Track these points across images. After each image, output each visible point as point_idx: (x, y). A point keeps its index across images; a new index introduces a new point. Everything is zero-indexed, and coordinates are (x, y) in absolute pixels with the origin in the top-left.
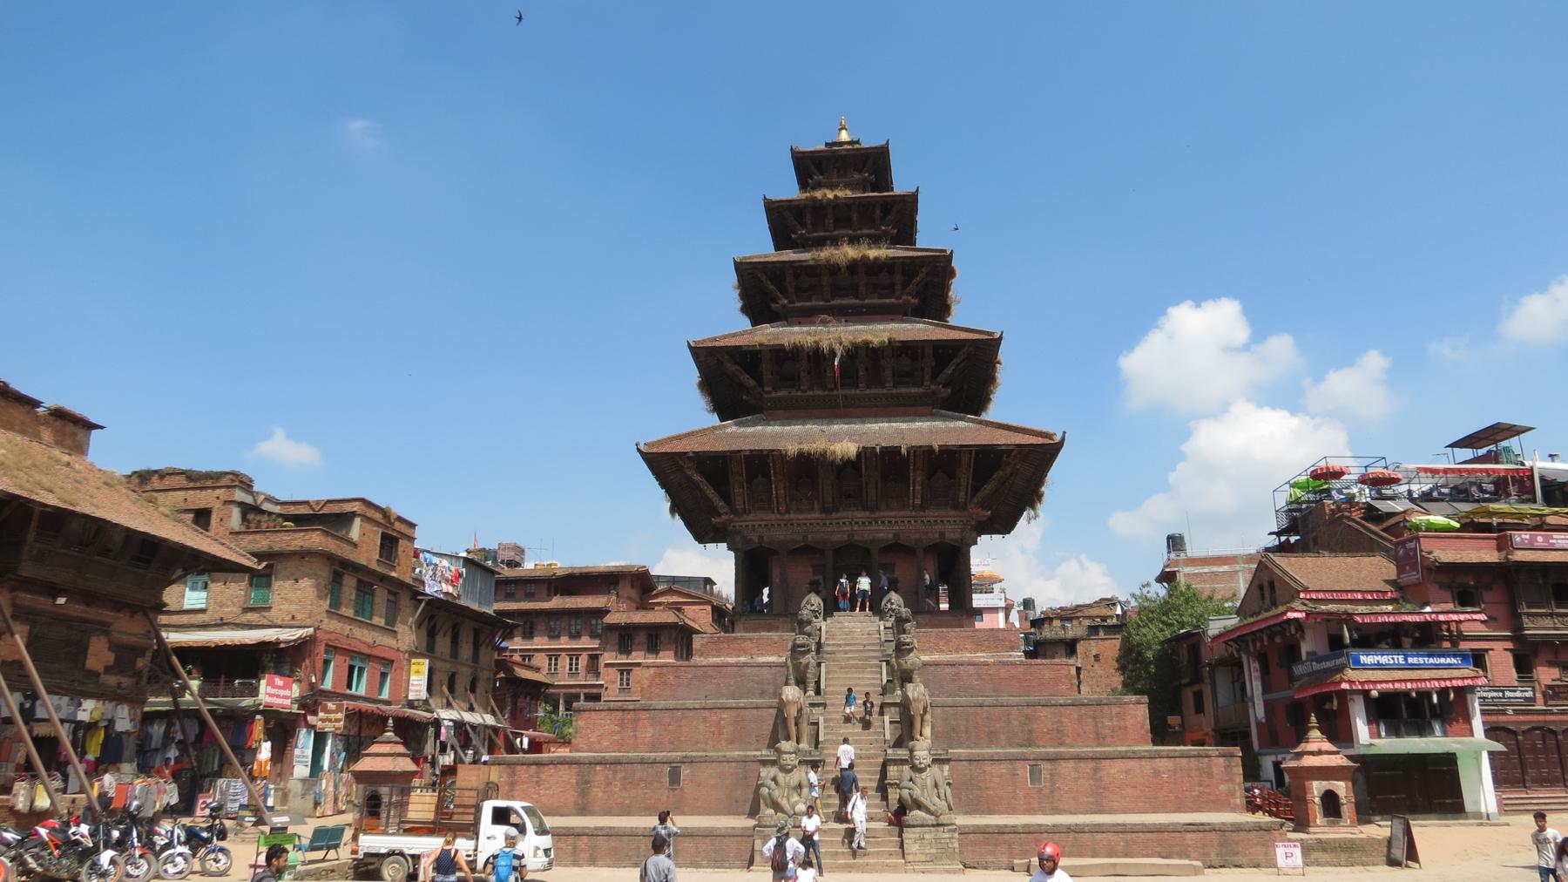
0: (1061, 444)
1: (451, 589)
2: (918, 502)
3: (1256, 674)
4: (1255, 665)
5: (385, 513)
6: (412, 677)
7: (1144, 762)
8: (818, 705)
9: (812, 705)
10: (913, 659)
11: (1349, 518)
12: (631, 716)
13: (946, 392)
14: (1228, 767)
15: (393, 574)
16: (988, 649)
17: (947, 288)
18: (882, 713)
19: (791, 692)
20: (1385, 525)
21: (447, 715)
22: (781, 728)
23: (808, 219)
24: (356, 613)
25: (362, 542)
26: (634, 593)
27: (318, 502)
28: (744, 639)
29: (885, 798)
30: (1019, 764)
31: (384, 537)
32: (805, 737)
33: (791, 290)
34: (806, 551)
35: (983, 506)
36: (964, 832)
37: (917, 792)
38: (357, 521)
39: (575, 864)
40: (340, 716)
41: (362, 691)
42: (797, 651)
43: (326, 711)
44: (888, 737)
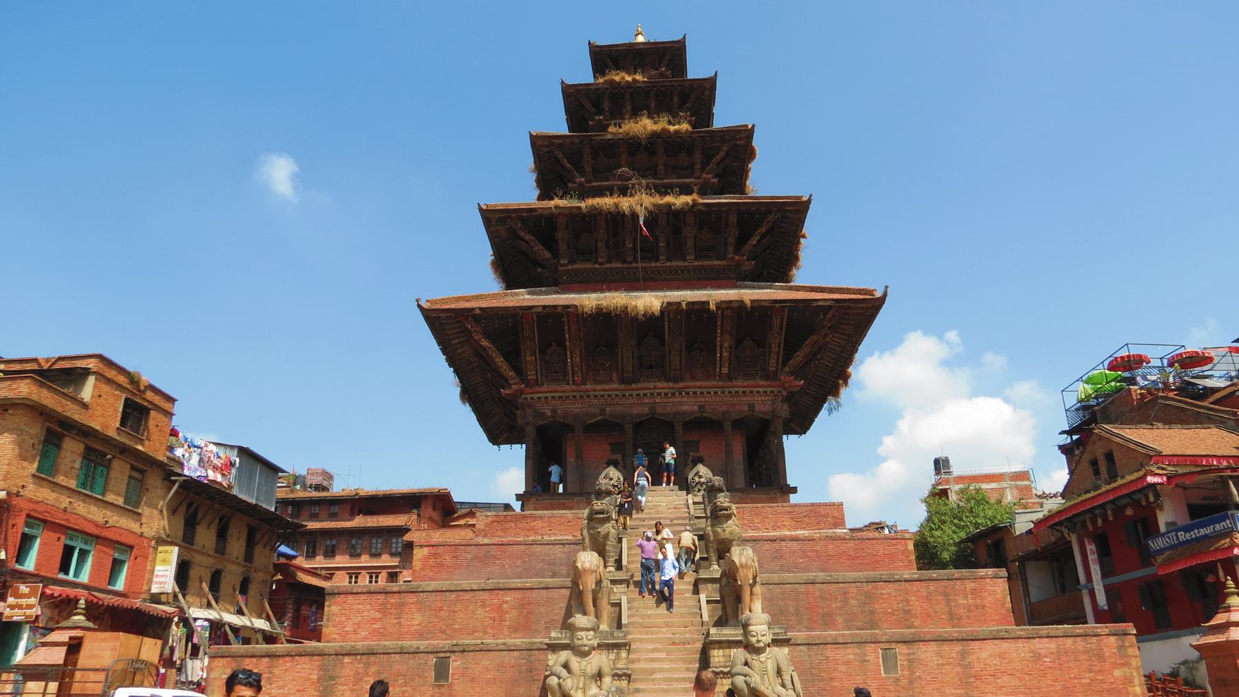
0: (882, 300)
1: (219, 478)
2: (725, 370)
3: (1092, 557)
4: (1091, 547)
5: (133, 379)
6: (157, 568)
7: (1020, 643)
8: (620, 582)
9: (614, 582)
10: (731, 527)
11: (1166, 398)
12: (394, 600)
13: (749, 265)
14: (1121, 647)
15: (140, 447)
18: (696, 591)
19: (588, 559)
20: (1211, 400)
21: (200, 615)
22: (576, 600)
23: (606, 105)
24: (84, 485)
25: (98, 407)
27: (47, 360)
30: (869, 648)
31: (128, 404)
32: (605, 617)
33: (588, 169)
34: (605, 427)
35: (798, 373)
37: (756, 680)
38: (91, 380)
40: (33, 601)
41: (84, 578)
42: (596, 519)
43: (17, 595)
44: (706, 618)
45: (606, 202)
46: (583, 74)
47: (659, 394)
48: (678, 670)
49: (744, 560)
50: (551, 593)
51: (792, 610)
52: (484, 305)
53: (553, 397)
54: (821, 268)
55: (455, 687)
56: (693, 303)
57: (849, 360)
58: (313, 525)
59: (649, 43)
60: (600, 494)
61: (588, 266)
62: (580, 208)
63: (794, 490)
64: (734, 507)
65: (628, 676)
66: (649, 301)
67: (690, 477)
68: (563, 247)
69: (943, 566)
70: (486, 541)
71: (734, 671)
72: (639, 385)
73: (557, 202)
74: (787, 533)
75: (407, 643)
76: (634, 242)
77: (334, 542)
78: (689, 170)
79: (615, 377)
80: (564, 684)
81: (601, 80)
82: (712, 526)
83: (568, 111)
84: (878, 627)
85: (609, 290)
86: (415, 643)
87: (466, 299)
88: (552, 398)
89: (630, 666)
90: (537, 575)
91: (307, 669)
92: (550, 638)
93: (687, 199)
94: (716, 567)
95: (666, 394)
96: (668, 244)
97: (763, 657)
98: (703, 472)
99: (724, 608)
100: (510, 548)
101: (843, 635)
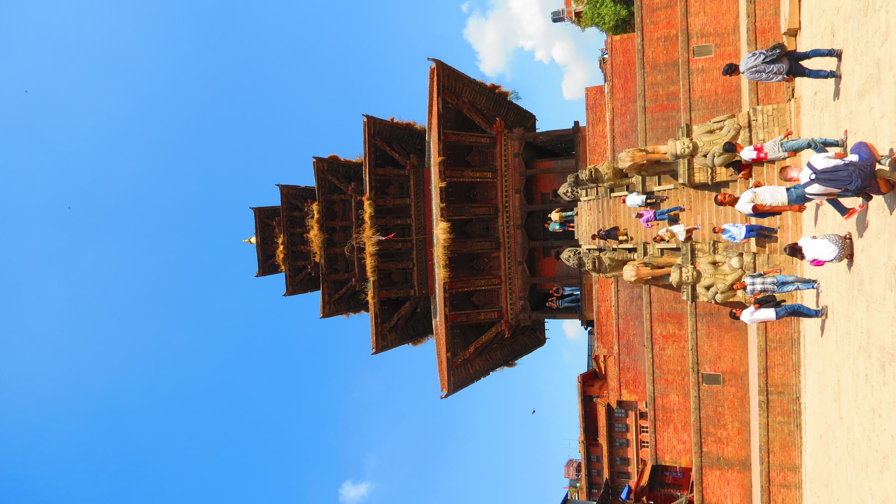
2: (490, 175)
8: (645, 249)
9: (645, 254)
10: (604, 169)
12: (660, 415)
13: (413, 158)
16: (603, 112)
17: (350, 162)
19: (629, 273)
22: (659, 281)
23: (301, 263)
26: (597, 385)
28: (599, 312)
30: (693, 67)
33: (346, 275)
35: (491, 122)
36: (757, 100)
37: (718, 149)
39: (799, 486)
42: (599, 267)
44: (671, 186)
45: (369, 263)
46: (279, 280)
47: (507, 222)
49: (628, 159)
50: (654, 299)
51: (665, 124)
52: (445, 350)
54: (414, 106)
55: (724, 369)
56: (441, 199)
57: (481, 86)
58: (606, 474)
59: (256, 234)
60: (581, 264)
61: (415, 276)
62: (374, 282)
63: (576, 123)
64: (589, 167)
65: (715, 242)
66: (440, 230)
67: (567, 199)
68: (402, 293)
69: (632, 14)
70: (616, 348)
71: (710, 165)
72: (501, 237)
73: (370, 298)
74: (608, 128)
75: (693, 406)
76: (398, 242)
77: (618, 459)
78: (346, 203)
79: (495, 255)
80: (721, 290)
81: (283, 268)
82: (603, 182)
83: (305, 291)
84: (677, 61)
85: (432, 259)
86: (692, 399)
87: (440, 363)
88: (511, 302)
89: (707, 240)
90: (641, 310)
91: (712, 478)
92: (688, 300)
93: (367, 204)
94: (634, 179)
95: (507, 217)
96: (399, 217)
97: (700, 144)
98: (564, 189)
99: (664, 173)
100: (621, 329)
101: (683, 85)
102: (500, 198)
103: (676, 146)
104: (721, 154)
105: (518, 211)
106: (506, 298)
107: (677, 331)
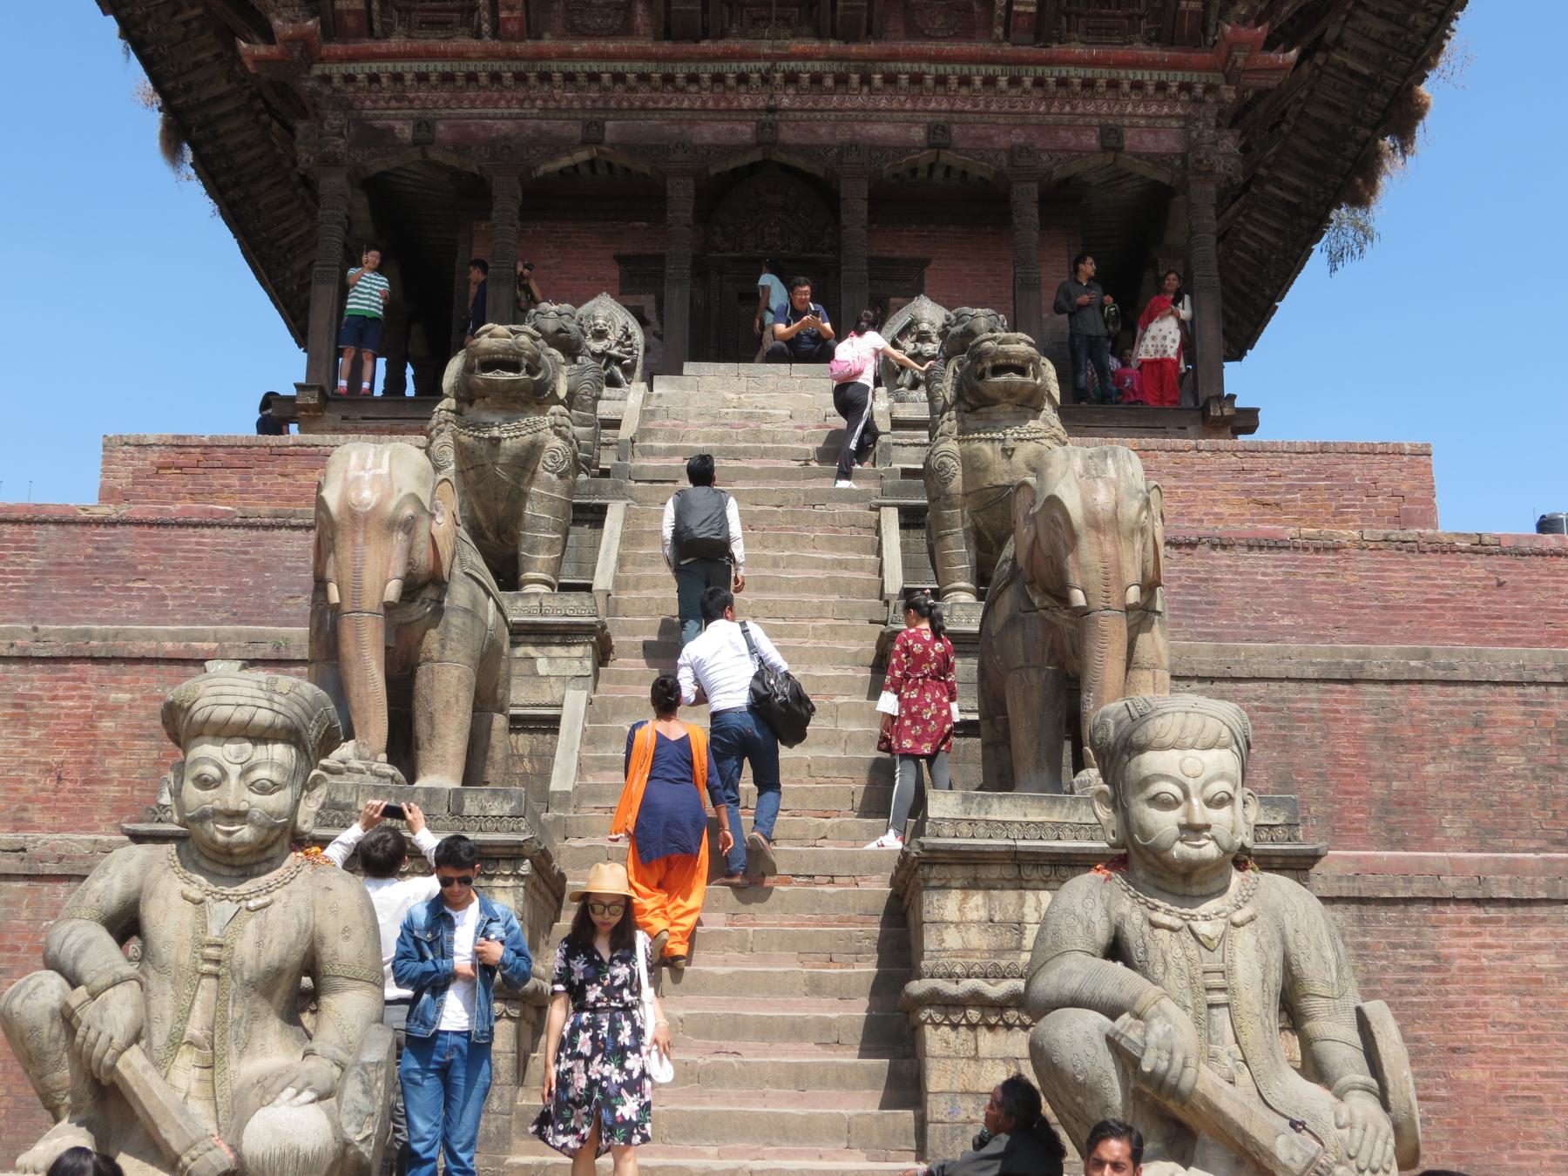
8: (565, 634)
29: (906, 1088)
37: (1170, 1035)
47: (791, 78)
48: (771, 986)
49: (1103, 498)
53: (422, 77)
72: (722, 44)
80: (88, 1014)
95: (816, 79)
97: (1209, 916)
100: (190, 537)
101: (1513, 869)
102: (915, 46)
103: (1195, 759)
104: (1126, 1058)
105: (843, 135)
106: (431, 55)
107: (113, 791)
